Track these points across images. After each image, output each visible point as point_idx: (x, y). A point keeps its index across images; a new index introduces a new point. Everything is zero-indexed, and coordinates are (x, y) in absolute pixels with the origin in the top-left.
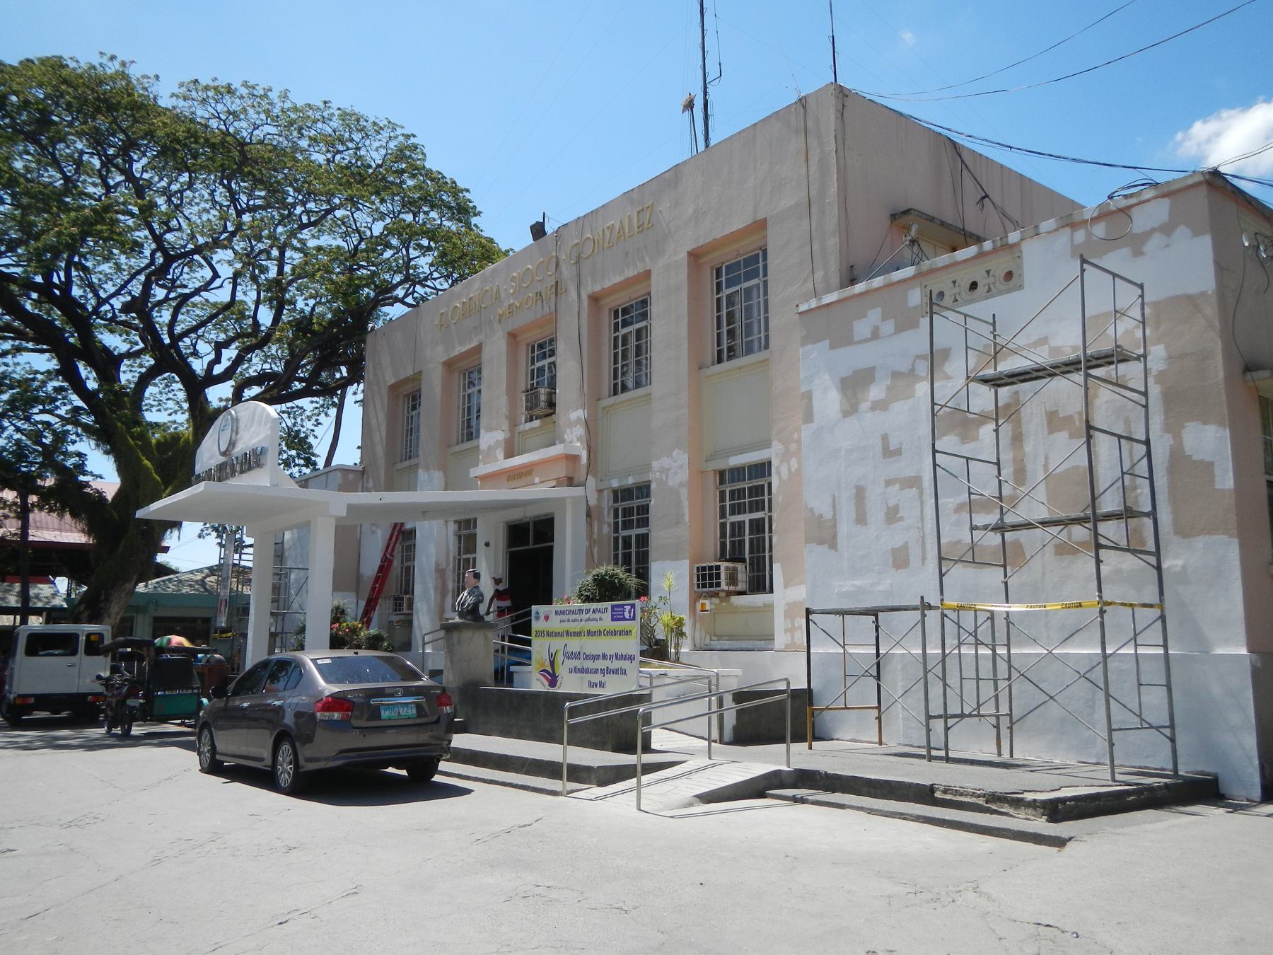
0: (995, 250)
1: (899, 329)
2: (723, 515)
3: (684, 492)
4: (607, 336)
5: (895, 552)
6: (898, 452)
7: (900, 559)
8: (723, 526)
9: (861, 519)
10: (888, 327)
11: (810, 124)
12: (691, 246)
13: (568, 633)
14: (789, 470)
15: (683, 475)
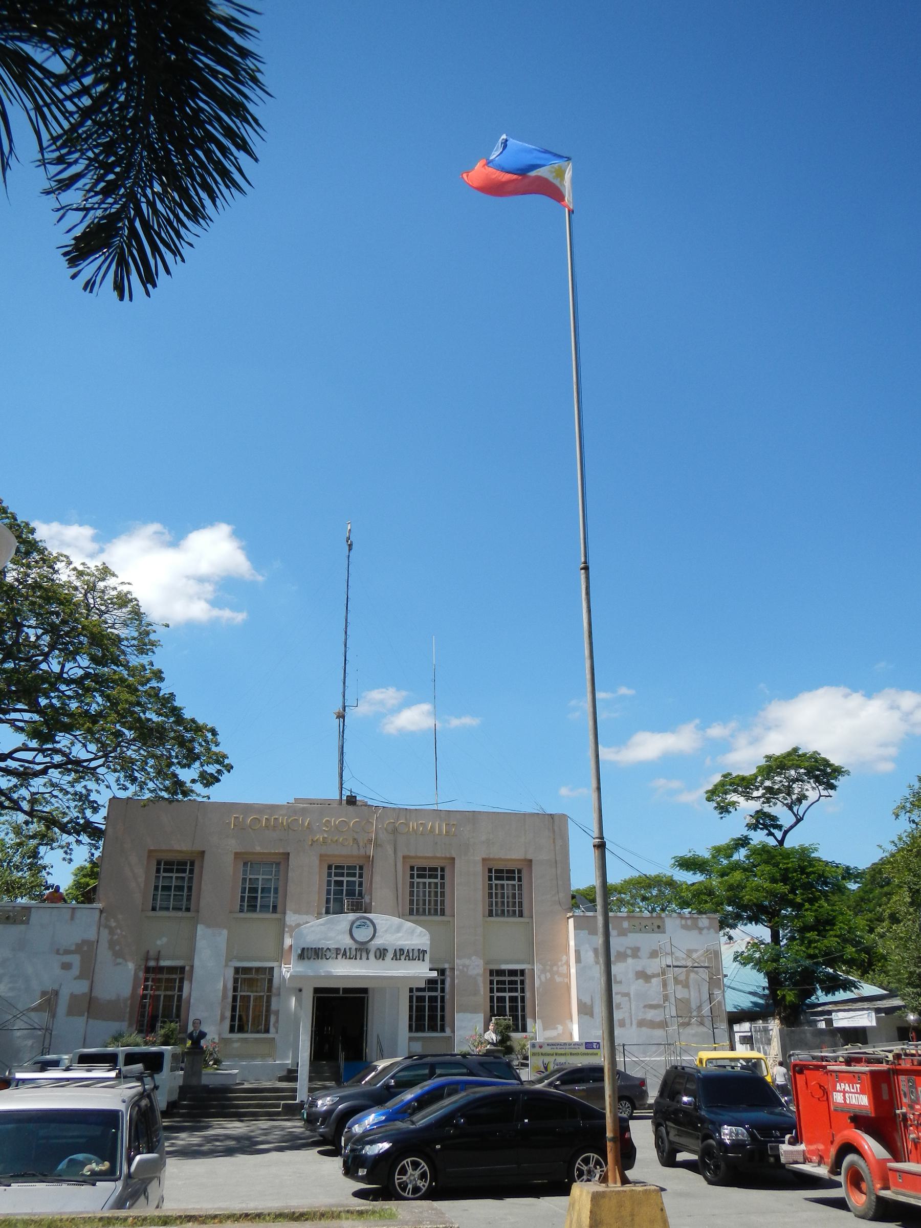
0: (656, 917)
2: (492, 990)
3: (480, 980)
4: (408, 880)
8: (492, 998)
11: (556, 828)
12: (484, 857)
13: (556, 1054)
14: (546, 977)
15: (481, 971)
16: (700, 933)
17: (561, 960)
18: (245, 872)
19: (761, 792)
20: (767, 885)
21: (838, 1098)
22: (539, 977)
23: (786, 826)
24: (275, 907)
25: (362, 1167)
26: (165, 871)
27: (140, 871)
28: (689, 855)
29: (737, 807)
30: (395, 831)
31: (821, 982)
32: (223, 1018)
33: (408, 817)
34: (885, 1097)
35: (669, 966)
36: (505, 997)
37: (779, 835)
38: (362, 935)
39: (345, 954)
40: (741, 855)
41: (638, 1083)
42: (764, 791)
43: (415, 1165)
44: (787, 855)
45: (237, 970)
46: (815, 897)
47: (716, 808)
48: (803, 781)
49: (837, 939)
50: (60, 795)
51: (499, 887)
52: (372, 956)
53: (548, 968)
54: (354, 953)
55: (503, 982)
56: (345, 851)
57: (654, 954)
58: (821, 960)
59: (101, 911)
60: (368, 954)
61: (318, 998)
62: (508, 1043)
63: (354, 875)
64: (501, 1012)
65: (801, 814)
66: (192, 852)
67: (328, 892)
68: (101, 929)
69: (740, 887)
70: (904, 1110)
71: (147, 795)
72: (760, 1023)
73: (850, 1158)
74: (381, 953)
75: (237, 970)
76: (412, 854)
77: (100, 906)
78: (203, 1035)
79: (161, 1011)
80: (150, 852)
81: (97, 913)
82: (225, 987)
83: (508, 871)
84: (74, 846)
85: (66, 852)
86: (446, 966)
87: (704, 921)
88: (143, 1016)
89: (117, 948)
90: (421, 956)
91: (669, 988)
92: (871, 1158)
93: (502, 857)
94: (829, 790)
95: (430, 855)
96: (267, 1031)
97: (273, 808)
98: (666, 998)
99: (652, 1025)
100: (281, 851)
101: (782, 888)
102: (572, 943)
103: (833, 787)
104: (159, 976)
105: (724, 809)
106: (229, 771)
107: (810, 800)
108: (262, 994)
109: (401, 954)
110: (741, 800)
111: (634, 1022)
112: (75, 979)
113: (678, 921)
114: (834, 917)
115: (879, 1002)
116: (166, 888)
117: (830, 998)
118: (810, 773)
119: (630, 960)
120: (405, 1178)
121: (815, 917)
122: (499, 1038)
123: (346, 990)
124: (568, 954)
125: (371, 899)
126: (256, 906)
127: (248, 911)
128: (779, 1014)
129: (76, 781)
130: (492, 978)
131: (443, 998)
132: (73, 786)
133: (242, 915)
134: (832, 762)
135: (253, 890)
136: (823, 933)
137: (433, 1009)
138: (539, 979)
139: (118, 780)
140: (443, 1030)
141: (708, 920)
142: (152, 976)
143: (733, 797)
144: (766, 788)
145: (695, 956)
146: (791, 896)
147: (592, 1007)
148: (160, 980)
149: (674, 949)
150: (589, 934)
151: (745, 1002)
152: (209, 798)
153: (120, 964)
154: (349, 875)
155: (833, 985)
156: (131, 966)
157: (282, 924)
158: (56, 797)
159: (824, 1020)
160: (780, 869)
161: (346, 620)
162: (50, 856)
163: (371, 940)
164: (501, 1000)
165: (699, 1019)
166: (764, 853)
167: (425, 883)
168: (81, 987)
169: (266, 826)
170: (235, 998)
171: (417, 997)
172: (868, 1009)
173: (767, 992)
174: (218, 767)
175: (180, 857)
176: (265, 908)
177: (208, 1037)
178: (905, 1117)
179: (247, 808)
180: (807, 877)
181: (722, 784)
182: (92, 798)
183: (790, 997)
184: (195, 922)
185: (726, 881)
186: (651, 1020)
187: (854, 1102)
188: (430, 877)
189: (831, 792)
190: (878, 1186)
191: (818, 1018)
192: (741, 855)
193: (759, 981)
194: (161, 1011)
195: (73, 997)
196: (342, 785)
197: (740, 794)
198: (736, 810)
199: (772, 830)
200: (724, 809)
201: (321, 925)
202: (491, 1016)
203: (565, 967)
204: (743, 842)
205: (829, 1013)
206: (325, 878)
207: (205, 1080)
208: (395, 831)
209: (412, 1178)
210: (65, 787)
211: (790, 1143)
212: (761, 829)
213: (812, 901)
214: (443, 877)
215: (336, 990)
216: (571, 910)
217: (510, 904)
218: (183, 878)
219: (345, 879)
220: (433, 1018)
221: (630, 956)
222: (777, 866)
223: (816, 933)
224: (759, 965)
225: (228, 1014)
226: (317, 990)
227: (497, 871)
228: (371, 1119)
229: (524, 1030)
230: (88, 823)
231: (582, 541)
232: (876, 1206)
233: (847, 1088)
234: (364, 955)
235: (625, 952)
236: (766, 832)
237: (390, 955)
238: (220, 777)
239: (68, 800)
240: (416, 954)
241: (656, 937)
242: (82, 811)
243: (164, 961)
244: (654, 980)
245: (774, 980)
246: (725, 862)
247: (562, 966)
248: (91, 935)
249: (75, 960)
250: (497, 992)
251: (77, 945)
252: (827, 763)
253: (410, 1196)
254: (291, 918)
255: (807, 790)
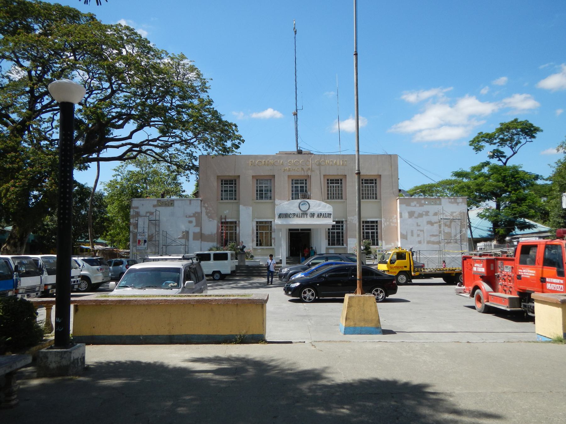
1: (420, 206)
4: (326, 185)
5: (419, 241)
6: (420, 226)
7: (420, 242)
9: (412, 235)
10: (418, 205)
16: (458, 205)
17: (394, 217)
18: (257, 183)
19: (498, 140)
20: (495, 183)
21: (475, 269)
22: (384, 224)
23: (508, 156)
24: (271, 197)
25: (290, 291)
26: (225, 184)
27: (215, 184)
28: (459, 171)
29: (484, 148)
30: (319, 165)
31: (517, 225)
32: (253, 241)
33: (325, 158)
34: (492, 269)
35: (442, 219)
36: (369, 232)
37: (504, 160)
38: (304, 208)
39: (297, 216)
40: (486, 170)
41: (421, 265)
42: (499, 140)
43: (309, 291)
44: (506, 170)
45: (257, 222)
46: (518, 188)
47: (474, 149)
48: (519, 135)
49: (526, 207)
50: (181, 154)
51: (366, 187)
52: (308, 216)
53: (388, 220)
54: (301, 215)
55: (369, 226)
56: (298, 173)
57: (436, 214)
58: (517, 215)
59: (201, 201)
60: (307, 215)
61: (290, 233)
62: (369, 250)
63: (303, 183)
64: (367, 238)
65: (516, 150)
66: (235, 176)
67: (292, 191)
68: (202, 207)
69: (482, 184)
70: (499, 274)
71: (214, 152)
72: (489, 243)
73: (478, 291)
74: (313, 215)
75: (257, 222)
76: (328, 174)
77: (200, 199)
78: (244, 247)
79: (229, 238)
80: (218, 176)
81: (200, 201)
82: (253, 229)
83: (371, 180)
84: (190, 175)
85: (187, 178)
86: (344, 220)
87: (460, 200)
88: (222, 240)
89: (209, 215)
90: (329, 216)
91: (442, 228)
92: (484, 291)
93: (368, 174)
94: (532, 139)
95: (336, 174)
96: (271, 245)
97: (267, 157)
98: (440, 232)
99: (433, 243)
100: (272, 174)
101: (501, 184)
102: (398, 210)
103: (534, 137)
104: (227, 225)
105: (478, 149)
106: (243, 143)
107: (522, 144)
108: (268, 231)
109: (320, 215)
110: (487, 145)
111: (425, 242)
112: (194, 227)
113: (448, 200)
114: (526, 197)
115: (544, 234)
116: (225, 191)
117: (522, 232)
118: (523, 130)
119: (424, 217)
120: (305, 295)
121: (517, 197)
122: (364, 248)
123: (302, 230)
124: (397, 214)
125: (311, 193)
126: (263, 197)
127: (259, 199)
128: (496, 238)
129: (187, 148)
130: (363, 224)
131: (342, 233)
132: (186, 150)
133: (257, 201)
134: (534, 125)
135: (261, 191)
136: (520, 204)
137: (338, 237)
138: (384, 225)
139: (203, 147)
140: (343, 245)
141: (461, 199)
142: (224, 225)
143: (483, 143)
144: (500, 139)
145: (454, 214)
146: (506, 188)
147: (407, 236)
148: (227, 227)
149: (444, 212)
150: (406, 206)
151: (485, 234)
152: (241, 153)
153: (210, 221)
154: (301, 183)
155: (524, 226)
156: (215, 222)
157: (274, 205)
158: (180, 155)
159: (517, 241)
160: (502, 176)
161: (296, 69)
162: (181, 179)
163: (308, 210)
164: (368, 233)
165: (455, 241)
166: (495, 169)
167: (334, 186)
168: (197, 230)
169: (264, 164)
170: (257, 233)
171: (331, 232)
172: (536, 236)
173: (492, 229)
174: (239, 141)
175: (230, 178)
176: (266, 198)
177: (247, 247)
178: (498, 276)
179: (256, 157)
180: (515, 180)
181: (478, 137)
182: (194, 155)
183: (502, 231)
184: (238, 204)
185: (475, 182)
186: (433, 241)
187: (480, 270)
188: (336, 183)
189: (533, 139)
190: (485, 301)
191: (514, 240)
192: (486, 170)
193: (488, 224)
194: (229, 238)
195: (194, 234)
196: (297, 145)
197: (487, 142)
198: (483, 149)
199: (500, 158)
200: (478, 149)
201: (287, 204)
202: (363, 239)
203: (395, 220)
204: (487, 164)
205: (518, 238)
206: (291, 185)
207: (247, 264)
208: (319, 165)
209: (308, 295)
210: (183, 151)
211: (459, 286)
212: (496, 158)
213: (515, 190)
214: (341, 183)
215: (298, 230)
216: (399, 196)
217: (372, 194)
218: (232, 187)
219: (299, 185)
220: (338, 240)
221: (424, 215)
222: (500, 174)
223: (516, 204)
224: (488, 217)
225: (255, 239)
226: (290, 230)
227: (365, 180)
228: (299, 275)
229: (377, 245)
230: (194, 165)
231: (355, 41)
232: (485, 308)
233: (478, 266)
234: (305, 216)
235: (422, 213)
236: (498, 159)
237: (316, 216)
238: (239, 145)
239: (185, 156)
240: (327, 215)
241: (437, 206)
242: (191, 160)
243: (228, 219)
244: (435, 225)
245: (496, 225)
246: (477, 173)
247: (394, 219)
248: (199, 210)
249: (193, 219)
250: (366, 230)
251: (193, 214)
252: (531, 125)
253: (308, 301)
254: (277, 202)
255: (521, 139)
